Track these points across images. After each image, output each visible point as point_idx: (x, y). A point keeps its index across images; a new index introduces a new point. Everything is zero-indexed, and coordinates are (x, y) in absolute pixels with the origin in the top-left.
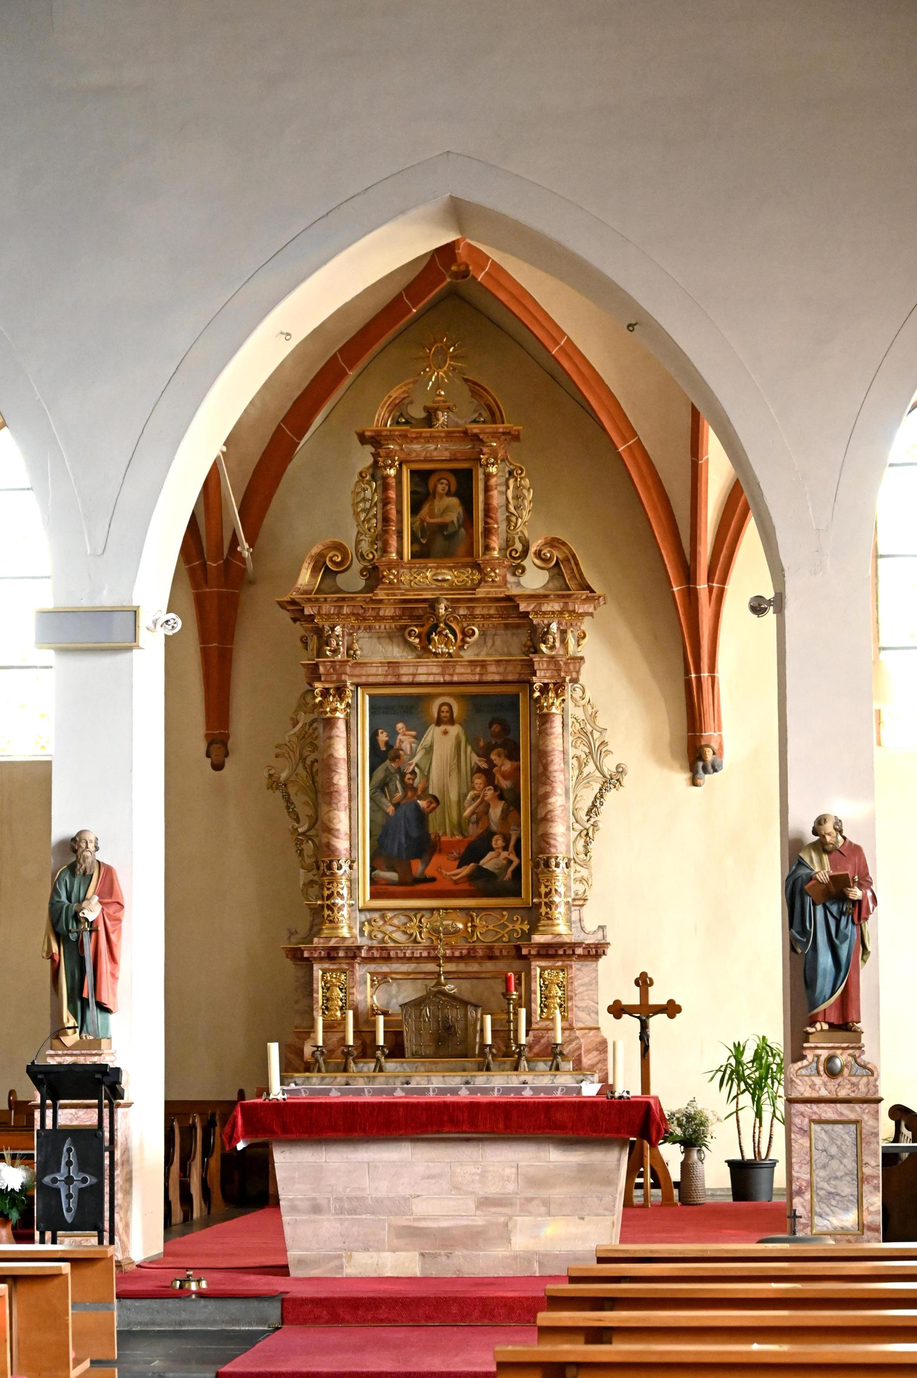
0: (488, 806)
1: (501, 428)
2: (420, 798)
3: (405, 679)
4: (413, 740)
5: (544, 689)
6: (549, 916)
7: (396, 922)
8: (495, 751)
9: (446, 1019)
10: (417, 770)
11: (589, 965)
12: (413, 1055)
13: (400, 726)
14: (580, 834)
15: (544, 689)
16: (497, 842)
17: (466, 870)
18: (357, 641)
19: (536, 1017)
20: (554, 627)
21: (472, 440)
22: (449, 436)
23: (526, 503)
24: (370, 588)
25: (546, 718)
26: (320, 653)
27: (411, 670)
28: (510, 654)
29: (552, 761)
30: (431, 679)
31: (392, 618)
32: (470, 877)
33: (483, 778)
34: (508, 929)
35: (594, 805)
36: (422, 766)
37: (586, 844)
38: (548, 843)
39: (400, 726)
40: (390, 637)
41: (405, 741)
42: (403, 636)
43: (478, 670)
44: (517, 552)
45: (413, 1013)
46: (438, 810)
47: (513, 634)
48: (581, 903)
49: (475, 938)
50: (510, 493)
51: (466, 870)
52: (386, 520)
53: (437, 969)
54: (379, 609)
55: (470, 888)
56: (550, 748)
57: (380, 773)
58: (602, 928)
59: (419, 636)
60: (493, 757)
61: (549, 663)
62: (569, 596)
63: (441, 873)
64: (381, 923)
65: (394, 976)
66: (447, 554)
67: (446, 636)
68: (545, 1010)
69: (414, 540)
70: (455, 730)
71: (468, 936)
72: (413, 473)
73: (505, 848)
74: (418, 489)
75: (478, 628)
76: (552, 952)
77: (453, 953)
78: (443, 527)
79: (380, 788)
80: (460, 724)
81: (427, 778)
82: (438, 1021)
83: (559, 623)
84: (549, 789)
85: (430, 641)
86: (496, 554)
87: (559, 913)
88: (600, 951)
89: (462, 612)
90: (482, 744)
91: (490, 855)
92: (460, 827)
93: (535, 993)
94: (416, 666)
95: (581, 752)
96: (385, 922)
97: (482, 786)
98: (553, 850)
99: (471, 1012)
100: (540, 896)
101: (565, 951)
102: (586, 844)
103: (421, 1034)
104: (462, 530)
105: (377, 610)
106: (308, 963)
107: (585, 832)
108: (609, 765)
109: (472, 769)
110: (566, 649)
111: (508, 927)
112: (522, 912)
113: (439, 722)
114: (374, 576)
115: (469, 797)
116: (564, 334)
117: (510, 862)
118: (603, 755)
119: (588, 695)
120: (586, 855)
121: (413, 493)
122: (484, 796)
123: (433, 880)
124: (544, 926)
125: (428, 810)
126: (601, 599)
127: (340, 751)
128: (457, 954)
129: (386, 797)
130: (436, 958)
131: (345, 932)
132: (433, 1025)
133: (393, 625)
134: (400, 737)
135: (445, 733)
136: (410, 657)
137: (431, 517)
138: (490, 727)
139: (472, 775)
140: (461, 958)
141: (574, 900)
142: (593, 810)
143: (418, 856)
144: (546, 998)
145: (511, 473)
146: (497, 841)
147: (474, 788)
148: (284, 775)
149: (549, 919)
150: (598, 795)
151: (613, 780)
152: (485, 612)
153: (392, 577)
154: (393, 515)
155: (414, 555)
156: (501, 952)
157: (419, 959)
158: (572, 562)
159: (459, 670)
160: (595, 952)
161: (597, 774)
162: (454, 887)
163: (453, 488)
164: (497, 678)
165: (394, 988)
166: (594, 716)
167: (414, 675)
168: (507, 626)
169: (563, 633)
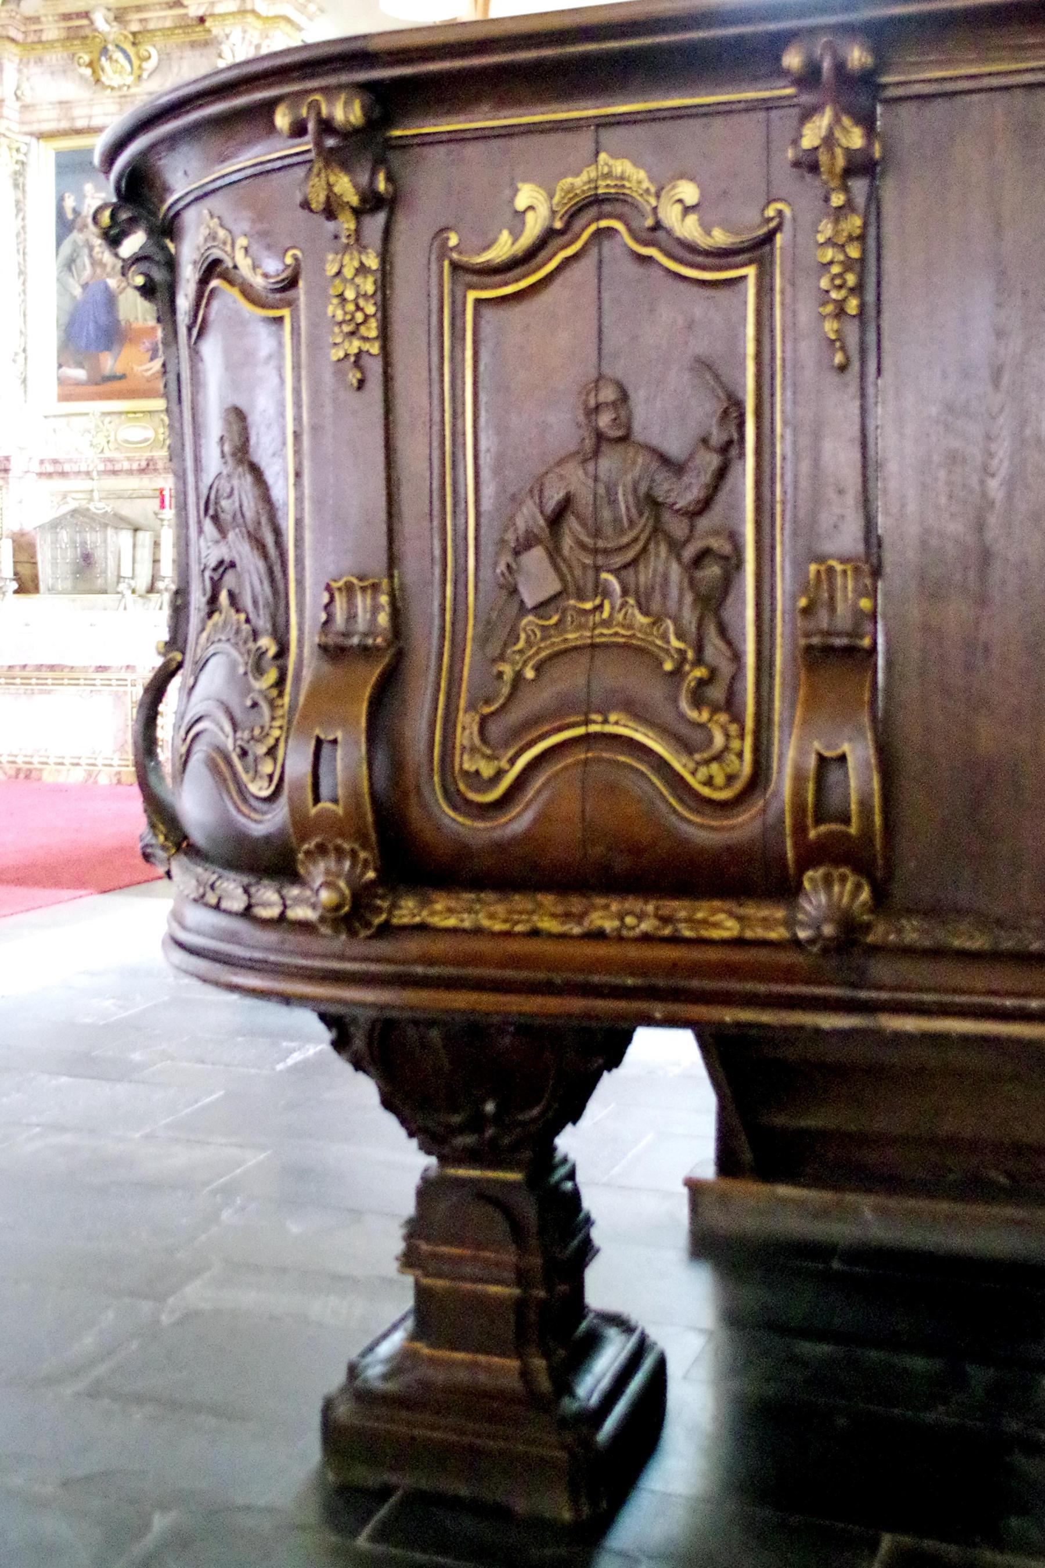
2: (109, 276)
3: (80, 124)
9: (84, 543)
18: (28, 79)
27: (86, 111)
47: (202, 55)
54: (41, 30)
59: (90, 65)
65: (74, 495)
82: (76, 547)
94: (91, 106)
103: (57, 563)
105: (38, 34)
123: (123, 377)
125: (118, 291)
129: (73, 276)
132: (70, 554)
143: (108, 348)
167: (90, 117)
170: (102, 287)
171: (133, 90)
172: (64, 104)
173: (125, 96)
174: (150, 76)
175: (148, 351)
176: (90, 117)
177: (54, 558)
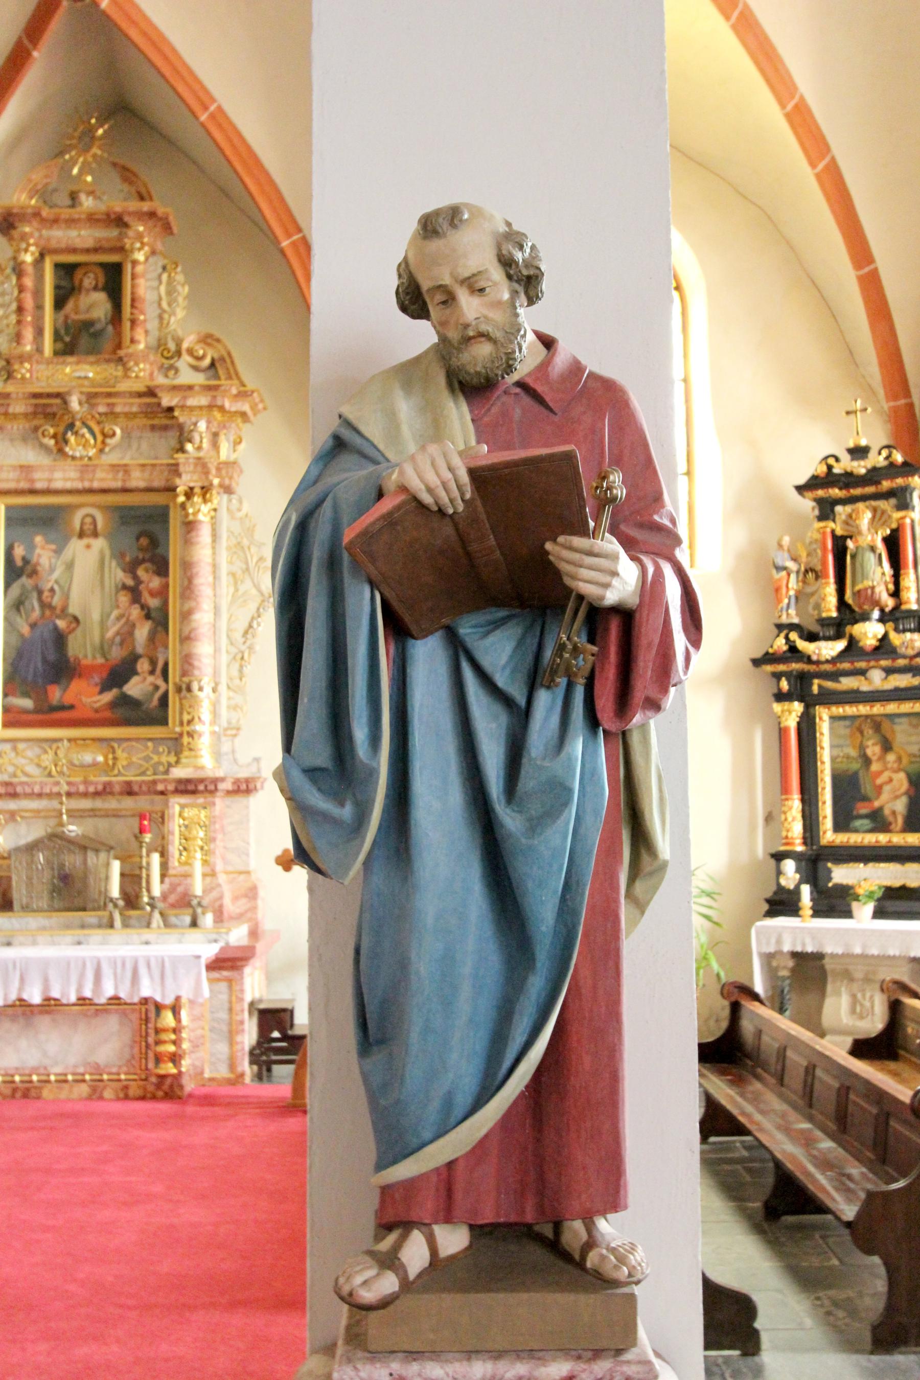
0: (134, 626)
1: (146, 206)
2: (58, 617)
3: (39, 485)
4: (52, 554)
6: (192, 747)
7: (29, 753)
8: (143, 566)
9: (62, 866)
10: (56, 587)
11: (240, 800)
12: (23, 908)
13: (38, 539)
14: (234, 658)
15: (189, 494)
16: (143, 665)
17: (108, 697)
19: (174, 863)
20: (202, 425)
21: (118, 226)
22: (92, 219)
23: (180, 299)
27: (46, 475)
28: (156, 458)
29: (197, 574)
30: (69, 485)
31: (26, 415)
32: (113, 705)
33: (129, 595)
34: (153, 762)
35: (250, 626)
36: (62, 582)
37: (241, 666)
38: (190, 664)
39: (38, 539)
40: (24, 440)
42: (38, 439)
43: (120, 475)
44: (169, 352)
45: (24, 858)
46: (79, 632)
48: (234, 732)
49: (116, 772)
50: (163, 289)
51: (108, 697)
53: (58, 806)
55: (114, 716)
56: (195, 559)
57: (16, 589)
58: (257, 760)
59: (54, 436)
60: (141, 572)
61: (196, 465)
62: (216, 388)
63: (81, 700)
64: (13, 755)
66: (93, 351)
67: (83, 436)
68: (184, 853)
69: (57, 337)
70: (99, 544)
71: (108, 768)
72: (58, 266)
73: (152, 672)
74: (63, 283)
75: (122, 429)
76: (191, 787)
77: (87, 788)
80: (105, 537)
81: (67, 596)
82: (53, 869)
83: (209, 422)
84: (192, 604)
85: (66, 442)
86: (142, 346)
87: (204, 743)
88: (251, 786)
89: (102, 409)
90: (128, 559)
91: (135, 680)
92: (103, 650)
93: (173, 834)
94: (52, 470)
95: (238, 566)
96: (17, 754)
97: (127, 604)
98: (196, 672)
99: (91, 857)
100: (181, 724)
101: (206, 786)
102: (241, 666)
104: (110, 328)
107: (239, 656)
109: (116, 586)
110: (218, 452)
111: (151, 758)
112: (170, 743)
113: (81, 535)
115: (113, 616)
116: (213, 100)
117: (157, 688)
118: (261, 572)
119: (246, 508)
120: (241, 679)
121: (57, 287)
122: (129, 615)
123: (72, 707)
124: (186, 757)
125: (67, 631)
126: (255, 395)
128: (91, 789)
129: (21, 616)
133: (27, 426)
134: (38, 551)
135: (88, 547)
136: (45, 460)
137: (76, 313)
138: (138, 539)
139: (117, 592)
140: (97, 794)
141: (226, 729)
144: (186, 839)
145: (164, 268)
146: (142, 664)
147: (118, 607)
149: (191, 750)
150: (256, 615)
152: (126, 409)
153: (23, 371)
154: (29, 303)
155: (56, 353)
156: (140, 787)
158: (228, 361)
159: (100, 474)
161: (254, 591)
162: (92, 715)
163: (100, 285)
164: (142, 484)
165: (23, 828)
167: (50, 480)
168: (153, 428)
169: (216, 435)
170: (51, 627)
171: (95, 462)
172: (26, 469)
173: (87, 466)
174: (110, 451)
175: (96, 685)
176: (50, 480)
177: (30, 879)
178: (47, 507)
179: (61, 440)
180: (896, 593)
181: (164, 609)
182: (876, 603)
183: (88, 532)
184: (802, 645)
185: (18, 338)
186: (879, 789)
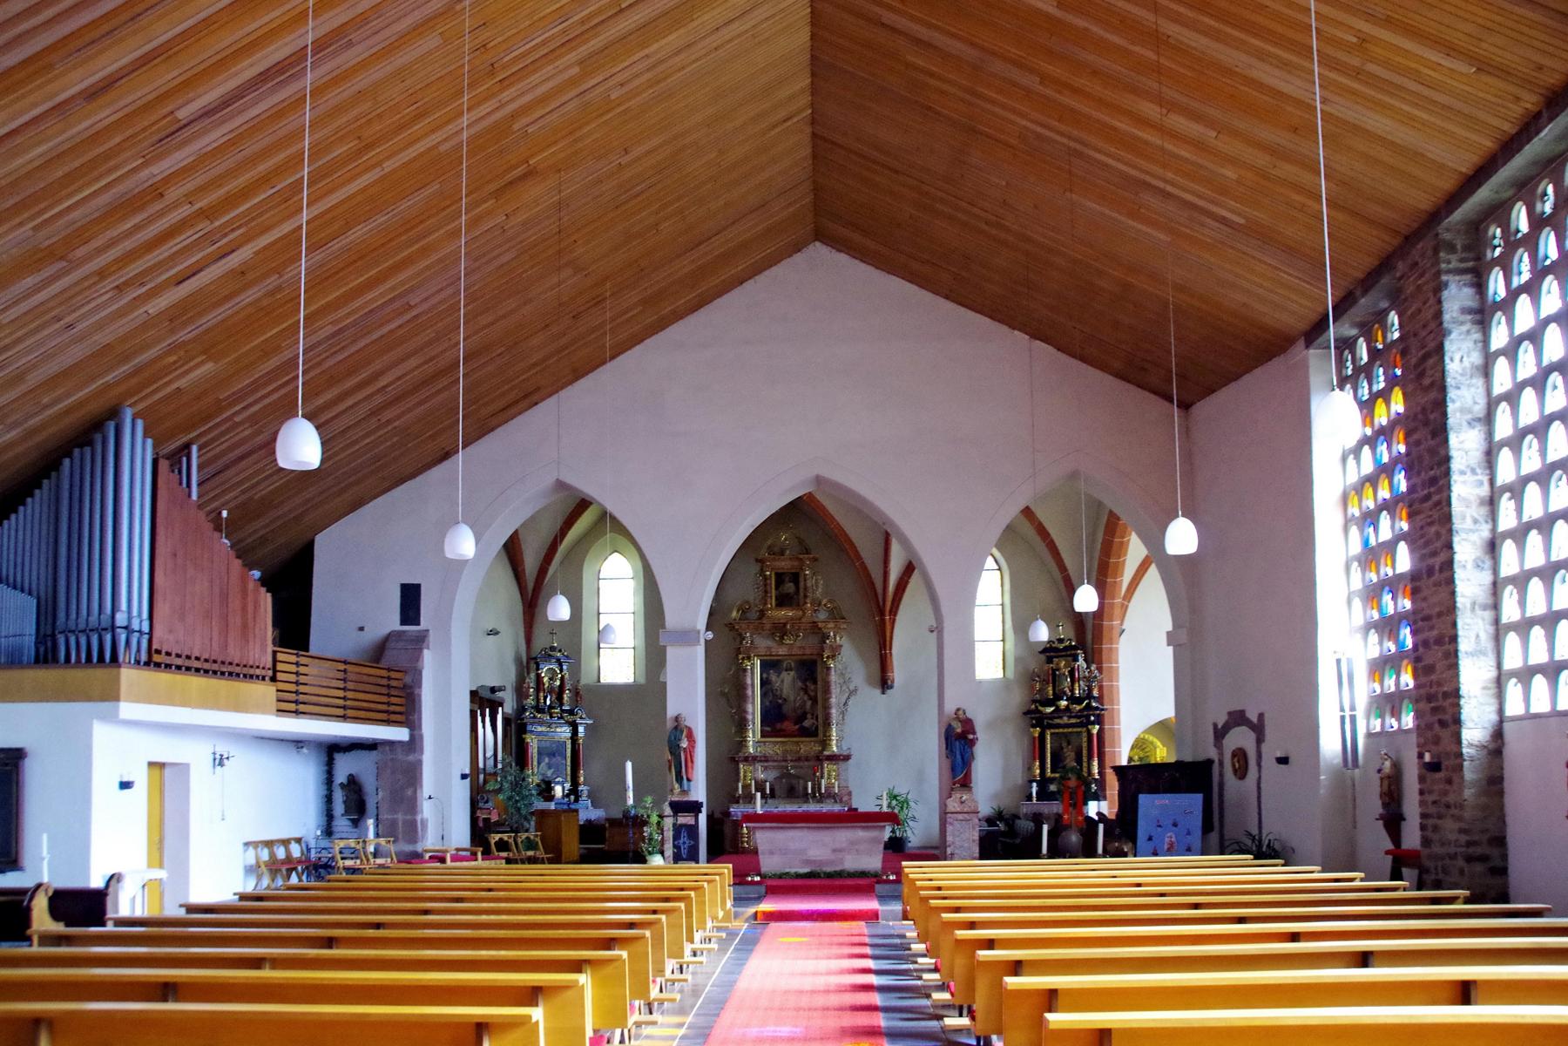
5: (828, 657)
16: (809, 716)
17: (797, 727)
20: (832, 634)
24: (760, 618)
25: (829, 669)
26: (741, 643)
32: (798, 729)
41: (773, 677)
51: (797, 727)
52: (766, 592)
69: (777, 599)
70: (792, 673)
78: (788, 594)
79: (763, 695)
81: (781, 690)
92: (795, 710)
106: (737, 763)
108: (852, 688)
114: (762, 614)
127: (749, 681)
130: (786, 761)
131: (751, 750)
140: (796, 760)
142: (845, 704)
148: (726, 691)
151: (853, 692)
155: (777, 605)
157: (780, 761)
160: (847, 758)
166: (846, 668)
172: (769, 648)
178: (773, 661)
179: (782, 638)
180: (1072, 690)
181: (816, 697)
182: (1065, 693)
183: (788, 669)
184: (1040, 708)
185: (765, 604)
186: (1066, 758)
